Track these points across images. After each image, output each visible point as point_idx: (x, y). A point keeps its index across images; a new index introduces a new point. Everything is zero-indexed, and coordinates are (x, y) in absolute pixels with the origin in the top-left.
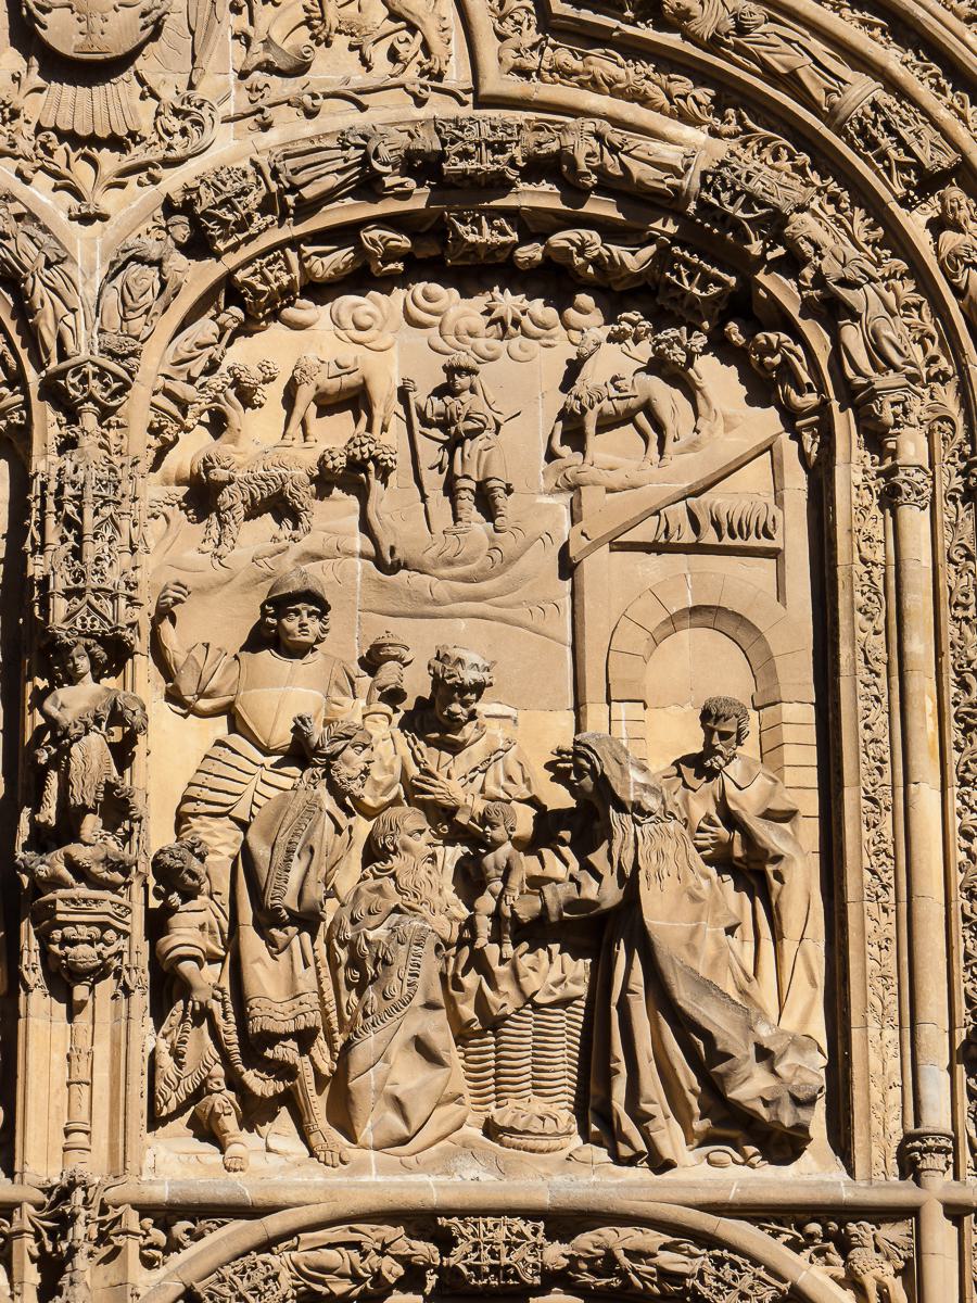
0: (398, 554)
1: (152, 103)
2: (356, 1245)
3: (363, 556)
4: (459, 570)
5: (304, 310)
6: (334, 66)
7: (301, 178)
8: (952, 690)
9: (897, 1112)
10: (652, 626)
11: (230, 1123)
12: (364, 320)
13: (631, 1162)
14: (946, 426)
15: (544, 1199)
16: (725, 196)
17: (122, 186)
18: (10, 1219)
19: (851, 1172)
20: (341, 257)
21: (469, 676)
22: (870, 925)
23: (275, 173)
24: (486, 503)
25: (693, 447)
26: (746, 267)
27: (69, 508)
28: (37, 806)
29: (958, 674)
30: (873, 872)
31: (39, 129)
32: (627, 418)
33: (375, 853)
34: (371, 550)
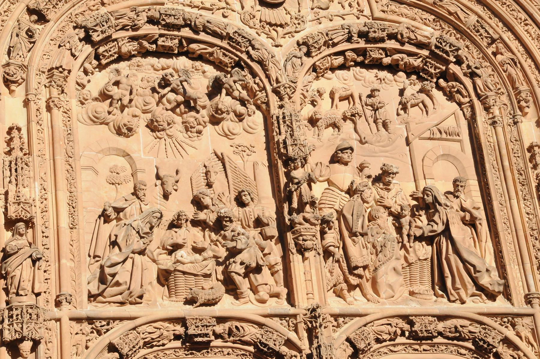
0: (366, 139)
1: (289, 16)
2: (390, 324)
3: (356, 140)
4: (381, 144)
5: (329, 74)
6: (335, 8)
7: (333, 37)
8: (516, 176)
9: (522, 288)
10: (433, 159)
11: (345, 292)
12: (346, 78)
13: (454, 301)
14: (505, 106)
15: (437, 312)
16: (444, 44)
17: (285, 38)
18: (296, 319)
19: (513, 304)
20: (340, 60)
21: (395, 170)
22: (506, 237)
23: (327, 35)
24: (385, 125)
25: (434, 113)
26: (446, 62)
27: (287, 123)
28: (290, 203)
29: (518, 171)
30: (505, 223)
31: (261, 21)
32: (417, 105)
33: (371, 218)
34: (359, 138)
